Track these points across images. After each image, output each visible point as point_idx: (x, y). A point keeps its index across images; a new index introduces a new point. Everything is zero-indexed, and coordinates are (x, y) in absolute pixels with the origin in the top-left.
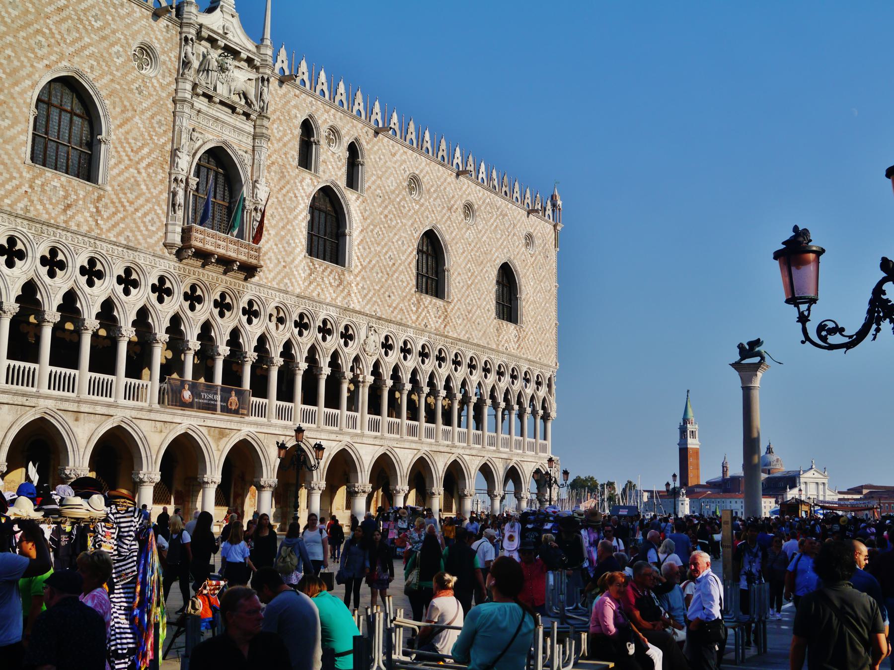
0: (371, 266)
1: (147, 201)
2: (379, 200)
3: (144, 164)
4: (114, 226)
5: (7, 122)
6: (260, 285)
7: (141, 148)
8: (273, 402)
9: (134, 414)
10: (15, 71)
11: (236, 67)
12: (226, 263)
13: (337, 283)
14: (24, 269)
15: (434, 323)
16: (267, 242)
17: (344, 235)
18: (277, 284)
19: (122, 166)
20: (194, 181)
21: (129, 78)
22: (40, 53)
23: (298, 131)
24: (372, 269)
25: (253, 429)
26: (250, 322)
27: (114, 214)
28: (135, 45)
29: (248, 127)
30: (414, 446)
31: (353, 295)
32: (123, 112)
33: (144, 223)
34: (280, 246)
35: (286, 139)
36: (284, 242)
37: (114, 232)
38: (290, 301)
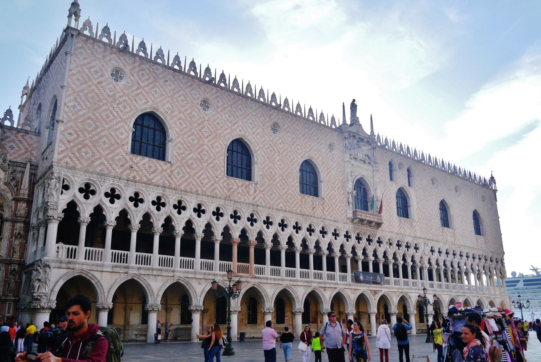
2: (422, 190)
3: (336, 188)
4: (329, 213)
6: (382, 231)
7: (335, 182)
8: (391, 278)
9: (344, 287)
10: (292, 160)
11: (364, 145)
12: (370, 222)
14: (302, 233)
15: (450, 239)
17: (410, 206)
19: (329, 190)
20: (355, 192)
21: (328, 156)
22: (299, 152)
23: (388, 167)
25: (386, 290)
26: (380, 246)
27: (329, 209)
28: (328, 143)
29: (370, 168)
30: (449, 293)
35: (384, 171)
37: (330, 216)
38: (394, 236)
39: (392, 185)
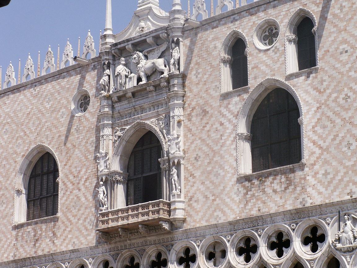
0: (337, 142)
1: (86, 208)
2: (344, 57)
4: (64, 240)
5: (5, 206)
7: (79, 172)
13: (283, 186)
16: (193, 186)
18: (207, 221)
24: (340, 143)
31: (309, 189)
32: (67, 153)
33: (84, 226)
34: (207, 183)
36: (212, 177)
37: (65, 244)
39: (229, 104)
